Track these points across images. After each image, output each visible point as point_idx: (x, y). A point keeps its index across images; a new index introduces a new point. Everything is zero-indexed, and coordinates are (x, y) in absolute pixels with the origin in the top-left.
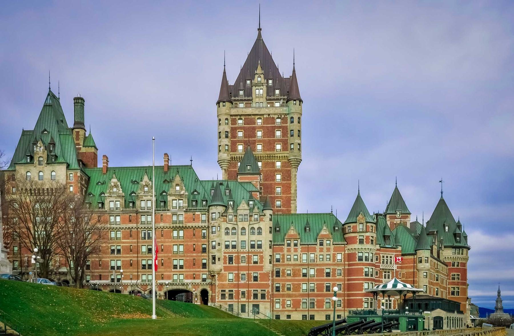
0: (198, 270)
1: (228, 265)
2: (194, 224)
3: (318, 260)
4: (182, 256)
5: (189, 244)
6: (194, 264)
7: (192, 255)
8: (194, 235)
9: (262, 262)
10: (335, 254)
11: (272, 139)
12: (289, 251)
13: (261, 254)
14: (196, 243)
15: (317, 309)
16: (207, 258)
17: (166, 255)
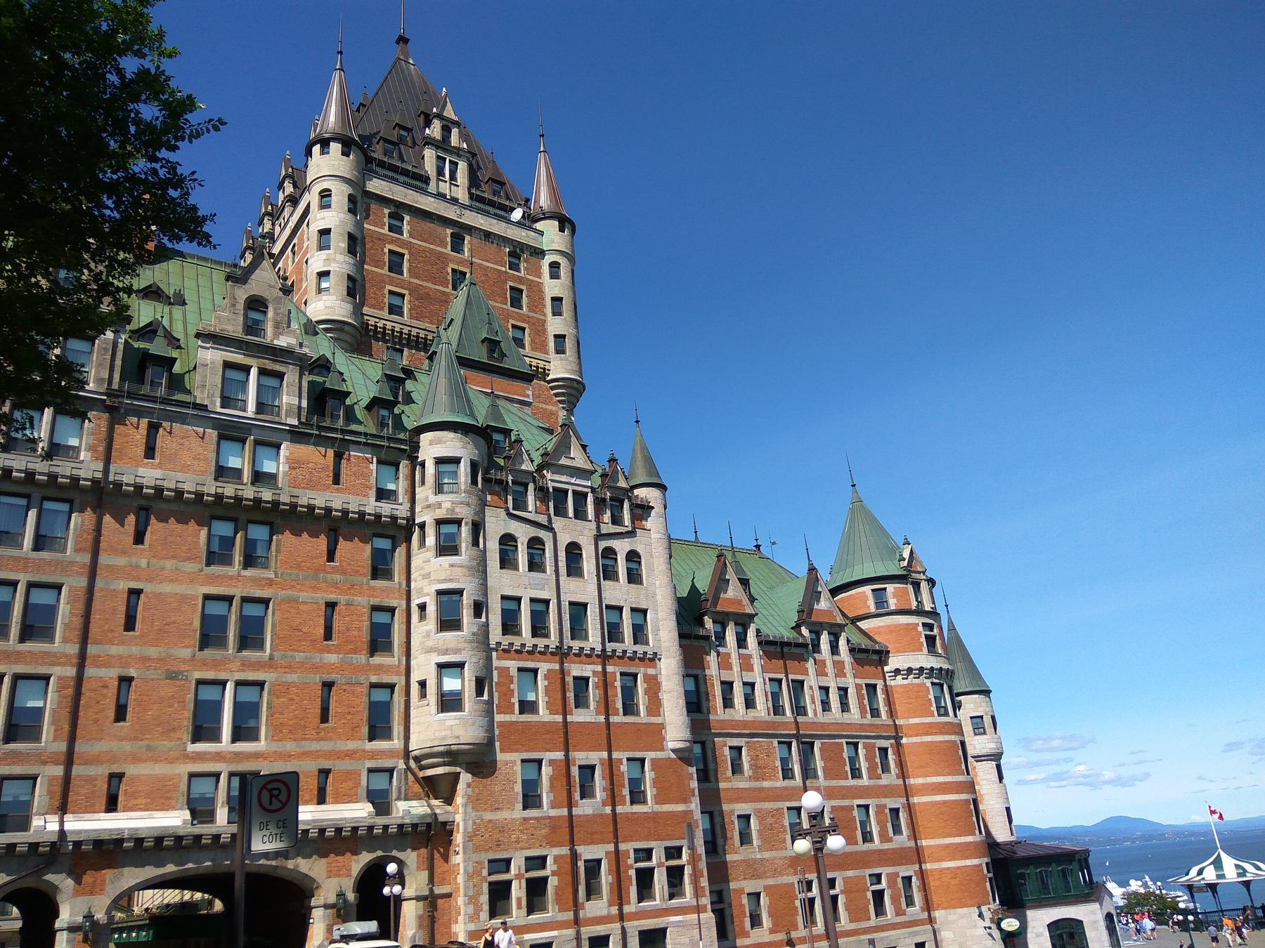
0: (351, 745)
1: (516, 717)
2: (337, 500)
3: (819, 708)
4: (258, 665)
5: (304, 596)
6: (324, 718)
7: (317, 657)
8: (331, 556)
9: (655, 706)
10: (861, 685)
11: (497, 305)
12: (725, 664)
13: (651, 671)
14: (342, 599)
15: (853, 926)
16: (399, 681)
17: (152, 652)
